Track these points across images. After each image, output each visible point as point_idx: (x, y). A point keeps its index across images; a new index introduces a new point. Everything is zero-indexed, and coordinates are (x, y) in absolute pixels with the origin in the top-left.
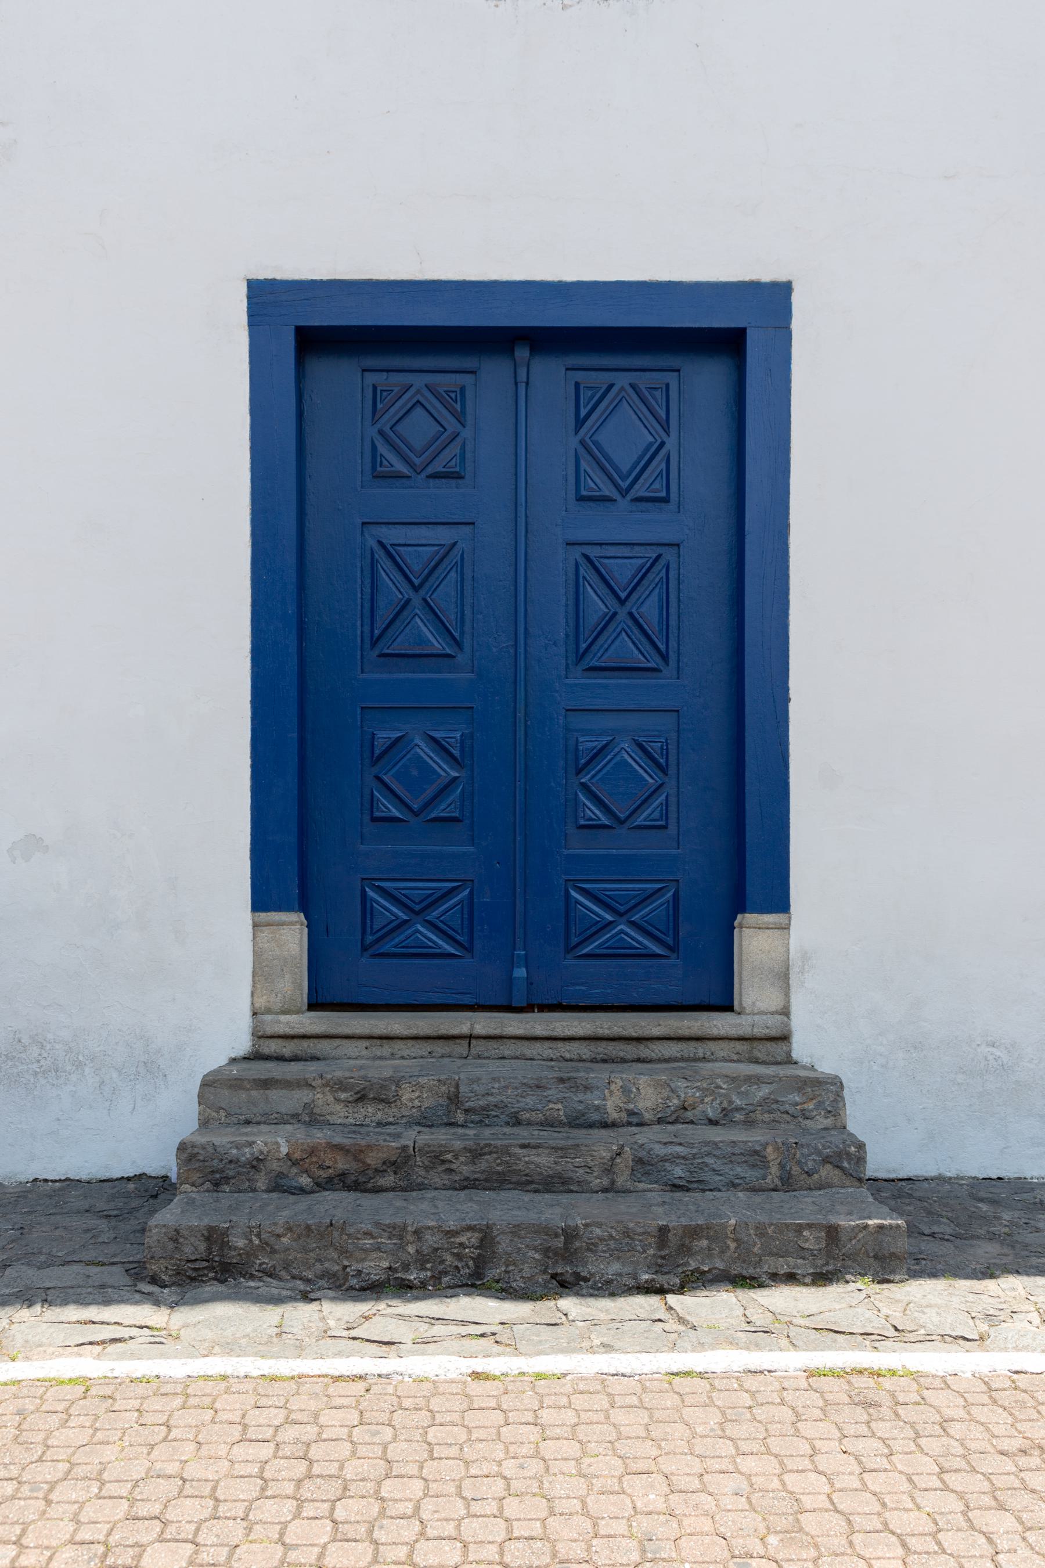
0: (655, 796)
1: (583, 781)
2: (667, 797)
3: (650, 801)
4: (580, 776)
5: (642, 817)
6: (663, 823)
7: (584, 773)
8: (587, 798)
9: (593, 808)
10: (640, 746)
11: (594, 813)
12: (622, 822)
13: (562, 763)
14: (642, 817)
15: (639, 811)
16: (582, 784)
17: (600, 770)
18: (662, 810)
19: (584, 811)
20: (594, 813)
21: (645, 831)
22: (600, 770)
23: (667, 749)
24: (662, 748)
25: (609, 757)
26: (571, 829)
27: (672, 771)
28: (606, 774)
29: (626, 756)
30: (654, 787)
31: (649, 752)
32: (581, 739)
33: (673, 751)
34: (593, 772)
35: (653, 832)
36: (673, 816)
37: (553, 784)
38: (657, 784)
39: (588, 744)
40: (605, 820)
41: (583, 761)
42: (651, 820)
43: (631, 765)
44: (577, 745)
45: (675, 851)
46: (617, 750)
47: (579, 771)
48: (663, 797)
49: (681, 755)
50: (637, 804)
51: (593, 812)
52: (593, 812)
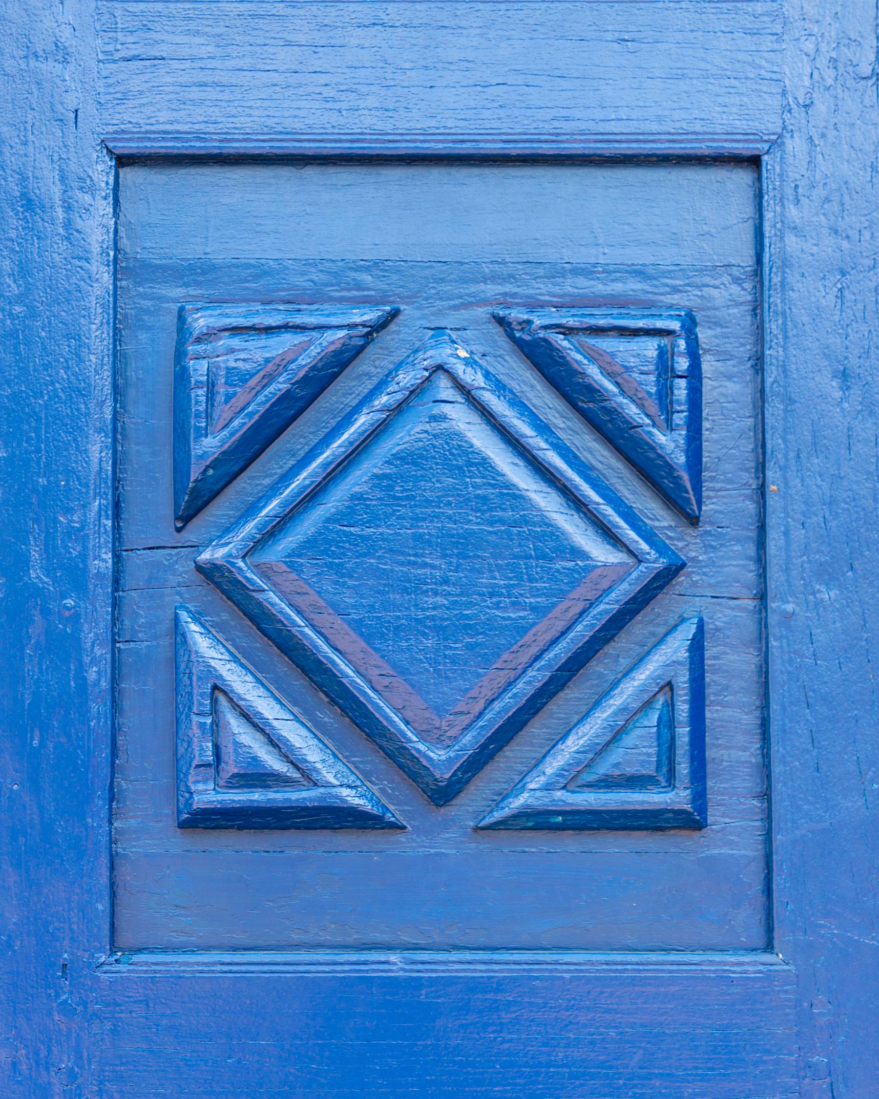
0: (624, 644)
1: (206, 556)
2: (697, 646)
3: (597, 667)
4: (191, 535)
5: (553, 766)
6: (678, 798)
7: (219, 511)
8: (244, 657)
9: (267, 708)
10: (541, 357)
11: (274, 742)
12: (443, 794)
13: (97, 451)
14: (553, 766)
15: (536, 729)
16: (211, 574)
17: (312, 496)
18: (668, 723)
19: (217, 726)
20: (274, 742)
21: (571, 844)
22: (312, 496)
23: (694, 375)
24: (664, 367)
25: (363, 421)
26: (147, 833)
27: (724, 499)
28: (344, 517)
29: (461, 419)
30: (624, 590)
31: (592, 391)
32: (200, 322)
33: (725, 389)
34: (273, 506)
35: (616, 846)
36: (732, 749)
37: (36, 574)
38: (639, 576)
39: (251, 360)
40: (339, 780)
41: (210, 445)
42: (607, 783)
43: (485, 463)
44: (180, 355)
45: (752, 963)
46: (407, 378)
47: (192, 505)
48: (676, 648)
49: (774, 410)
50: (524, 688)
51: (277, 732)
52: (277, 732)
